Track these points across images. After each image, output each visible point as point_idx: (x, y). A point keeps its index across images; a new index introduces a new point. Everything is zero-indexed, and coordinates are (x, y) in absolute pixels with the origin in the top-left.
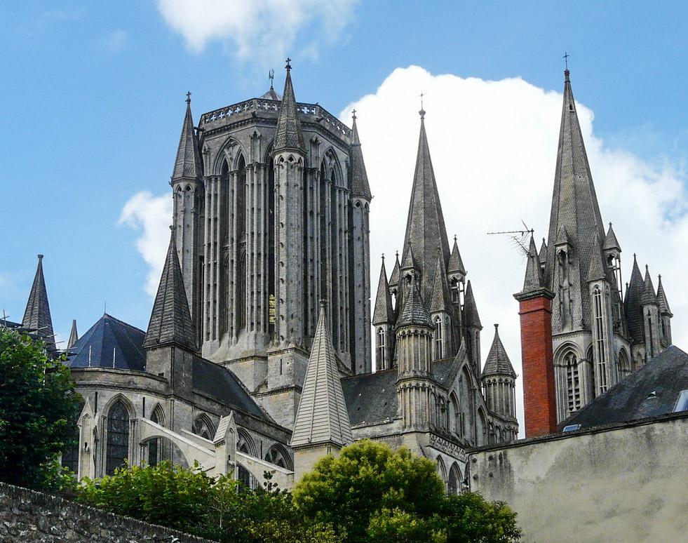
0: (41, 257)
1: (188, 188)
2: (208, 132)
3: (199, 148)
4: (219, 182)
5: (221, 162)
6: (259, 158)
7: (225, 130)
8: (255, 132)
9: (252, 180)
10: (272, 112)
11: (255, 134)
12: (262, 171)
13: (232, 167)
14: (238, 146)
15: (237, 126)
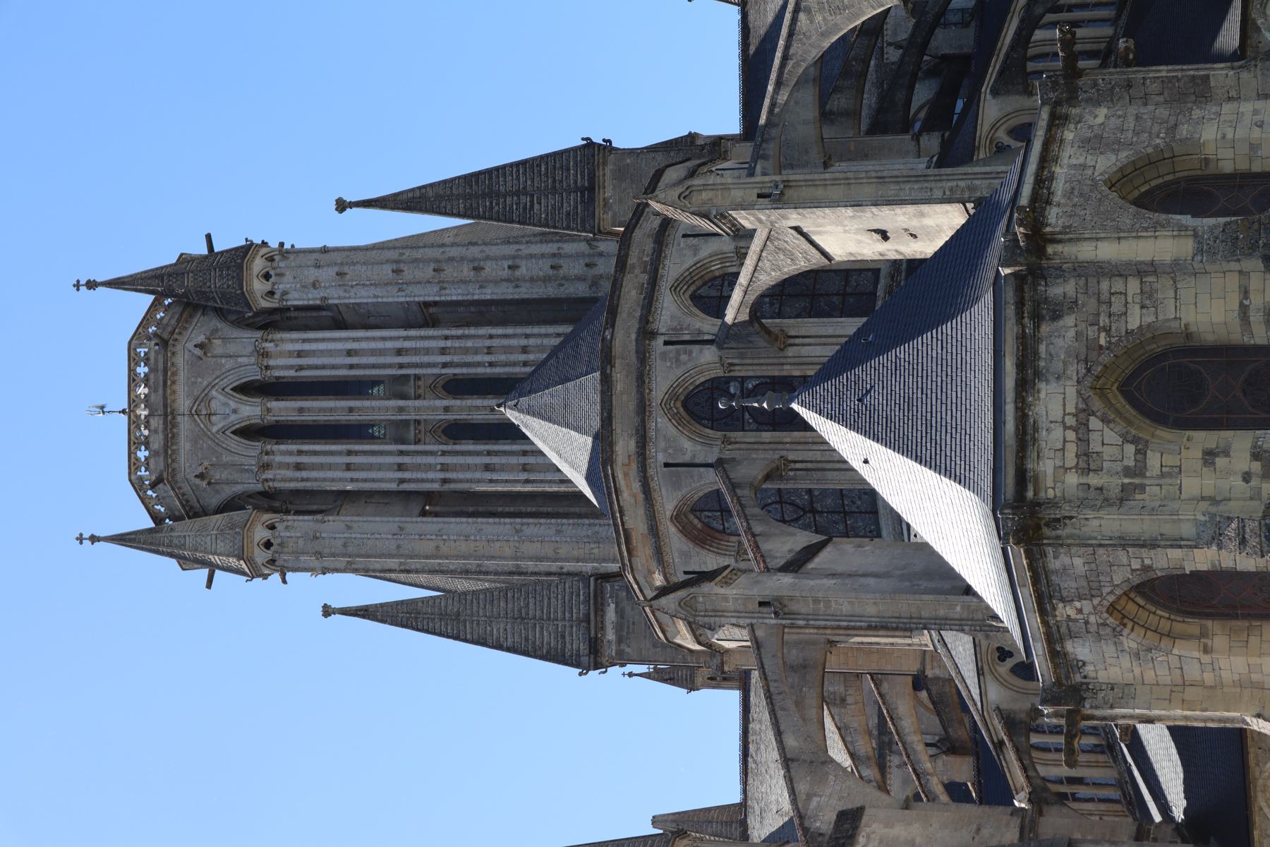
0: (327, 611)
1: (272, 527)
2: (167, 466)
3: (194, 511)
5: (236, 443)
6: (245, 340)
7: (174, 425)
9: (290, 354)
11: (200, 346)
12: (278, 336)
13: (251, 410)
14: (214, 393)
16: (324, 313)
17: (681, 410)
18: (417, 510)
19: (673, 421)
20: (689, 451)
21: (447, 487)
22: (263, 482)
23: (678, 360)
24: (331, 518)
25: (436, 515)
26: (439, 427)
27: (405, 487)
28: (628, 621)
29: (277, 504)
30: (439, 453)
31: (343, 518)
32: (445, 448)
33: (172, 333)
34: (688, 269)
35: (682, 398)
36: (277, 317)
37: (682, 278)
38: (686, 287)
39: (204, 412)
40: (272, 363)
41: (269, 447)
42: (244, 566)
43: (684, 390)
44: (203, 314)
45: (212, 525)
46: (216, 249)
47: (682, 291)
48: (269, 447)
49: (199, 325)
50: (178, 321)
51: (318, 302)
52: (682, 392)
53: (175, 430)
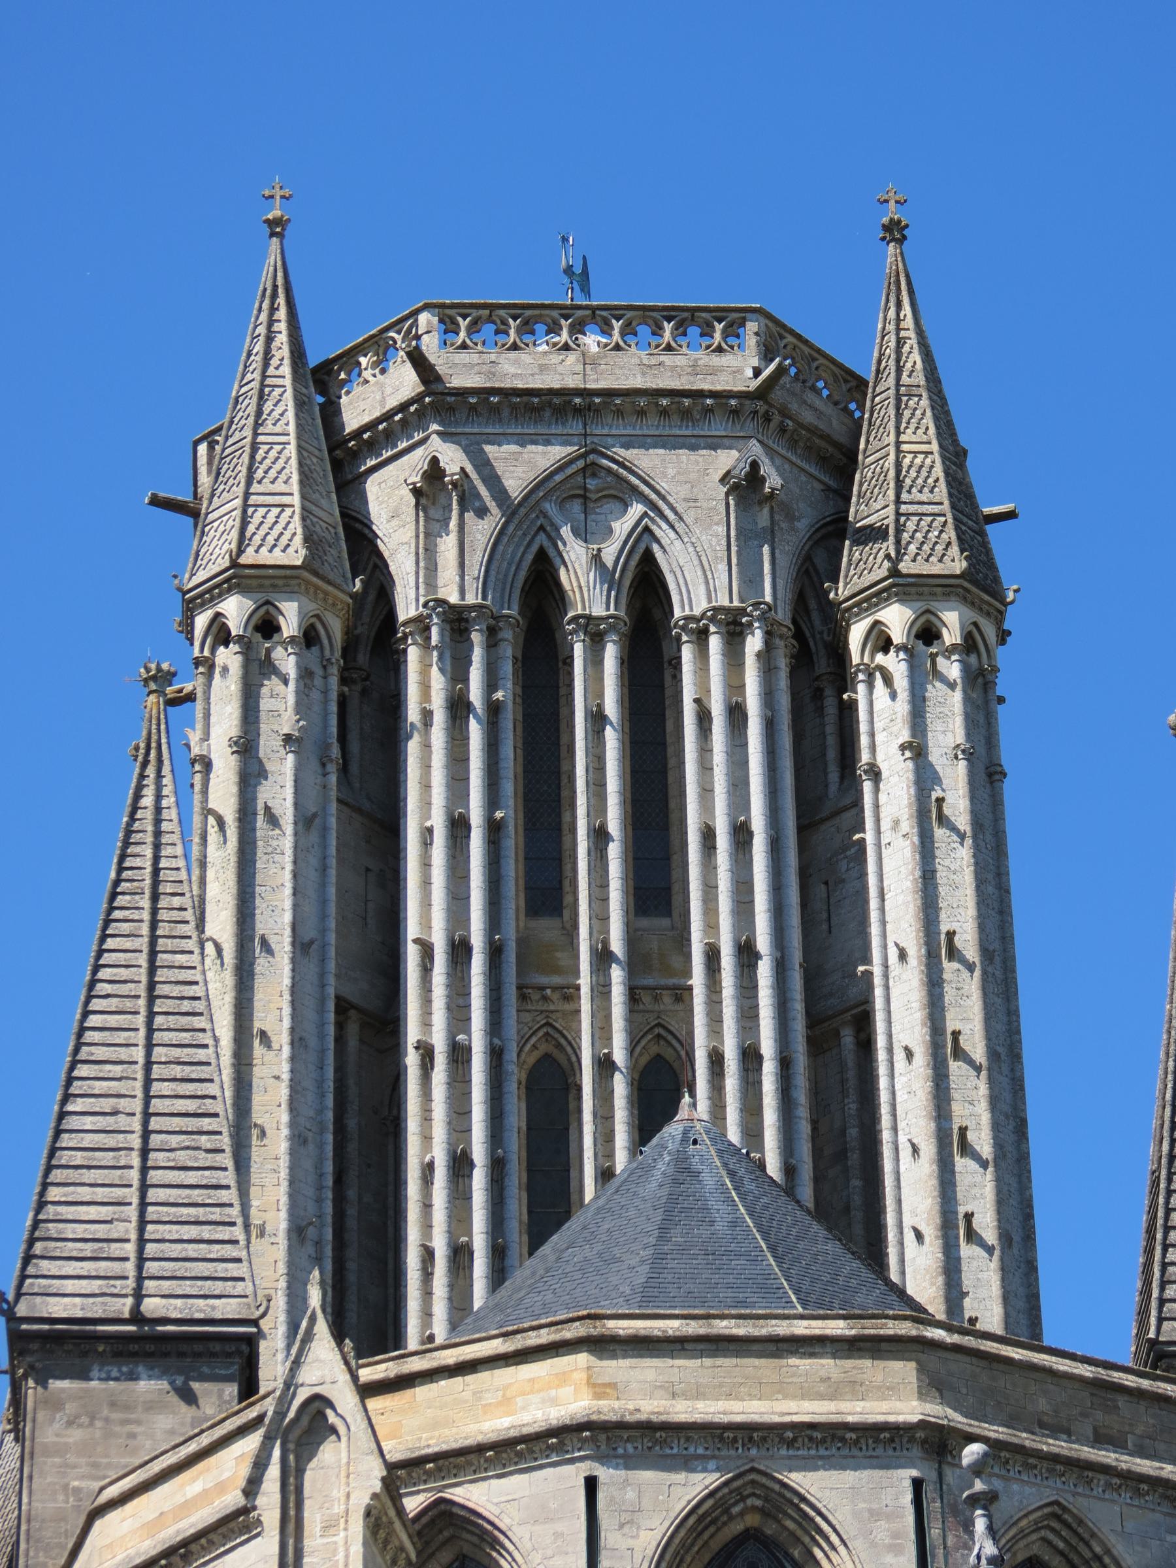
4: (508, 651)
8: (755, 465)
10: (810, 397)
11: (754, 476)
14: (637, 509)
15: (641, 413)
16: (834, 776)
17: (737, 1527)
18: (352, 993)
19: (710, 1502)
20: (631, 1543)
21: (412, 1059)
22: (418, 619)
23: (875, 1515)
24: (333, 778)
25: (340, 1039)
26: (559, 1046)
27: (412, 954)
28: (138, 1422)
29: (362, 658)
30: (496, 1041)
31: (333, 807)
32: (511, 1054)
33: (785, 413)
34: (1108, 1552)
35: (770, 1529)
36: (822, 665)
37: (1086, 1536)
38: (1061, 1545)
39: (592, 484)
40: (715, 643)
41: (507, 634)
42: (214, 569)
43: (792, 1534)
44: (828, 489)
45: (316, 496)
46: (990, 529)
47: (1051, 1536)
48: (507, 634)
49: (803, 478)
50: (812, 430)
51: (865, 757)
52: (786, 1528)
53: (547, 414)
